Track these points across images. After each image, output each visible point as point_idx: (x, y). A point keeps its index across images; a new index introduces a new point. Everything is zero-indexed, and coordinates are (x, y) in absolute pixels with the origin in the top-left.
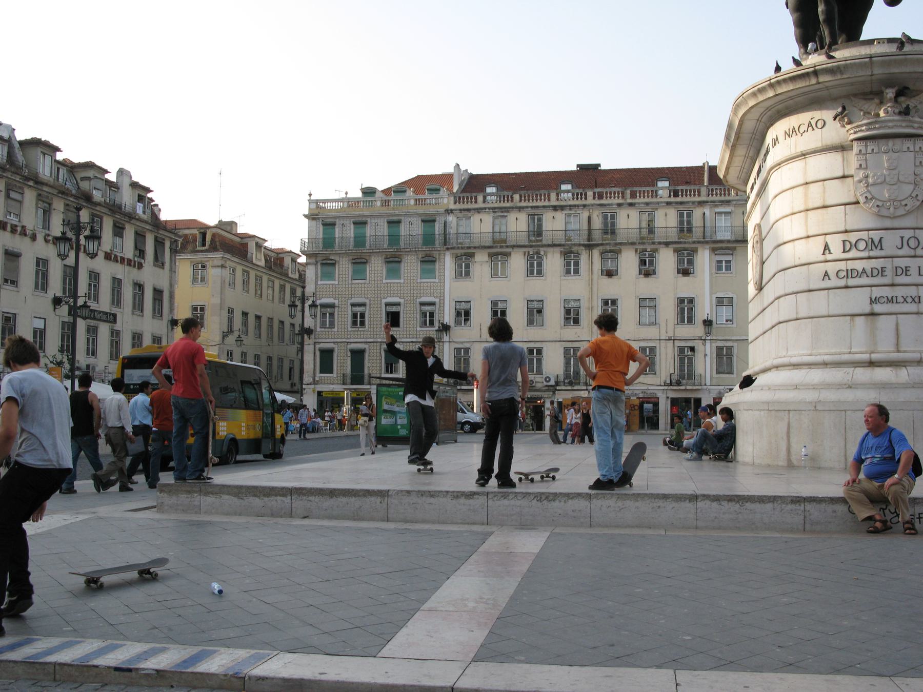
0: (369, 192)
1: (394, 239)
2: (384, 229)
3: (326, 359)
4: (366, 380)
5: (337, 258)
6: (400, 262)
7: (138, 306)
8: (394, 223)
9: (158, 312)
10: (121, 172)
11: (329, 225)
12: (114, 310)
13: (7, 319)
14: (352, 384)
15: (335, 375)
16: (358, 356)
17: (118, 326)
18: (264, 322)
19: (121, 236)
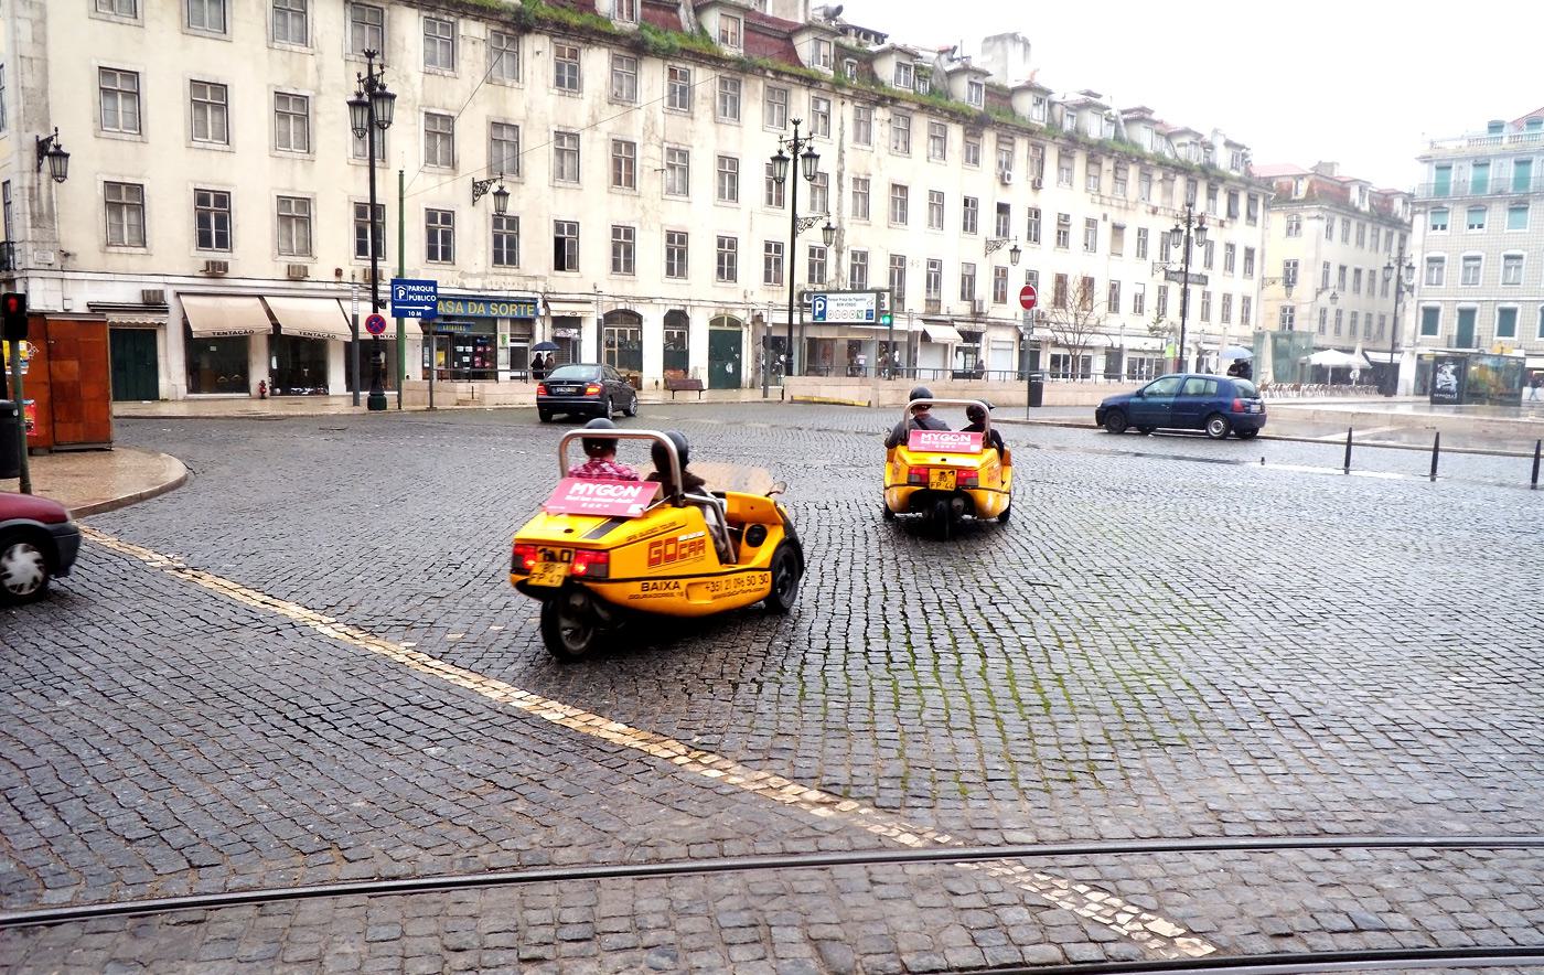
0: (1496, 127)
1: (1522, 181)
2: (1509, 171)
3: (1430, 319)
4: (1474, 344)
5: (1451, 207)
6: (1526, 209)
7: (1229, 266)
8: (1523, 163)
9: (1249, 270)
10: (1215, 132)
11: (1444, 168)
12: (1206, 272)
13: (1113, 287)
14: (1458, 347)
15: (1439, 337)
16: (1467, 316)
17: (1208, 288)
18: (1365, 276)
19: (1214, 198)
